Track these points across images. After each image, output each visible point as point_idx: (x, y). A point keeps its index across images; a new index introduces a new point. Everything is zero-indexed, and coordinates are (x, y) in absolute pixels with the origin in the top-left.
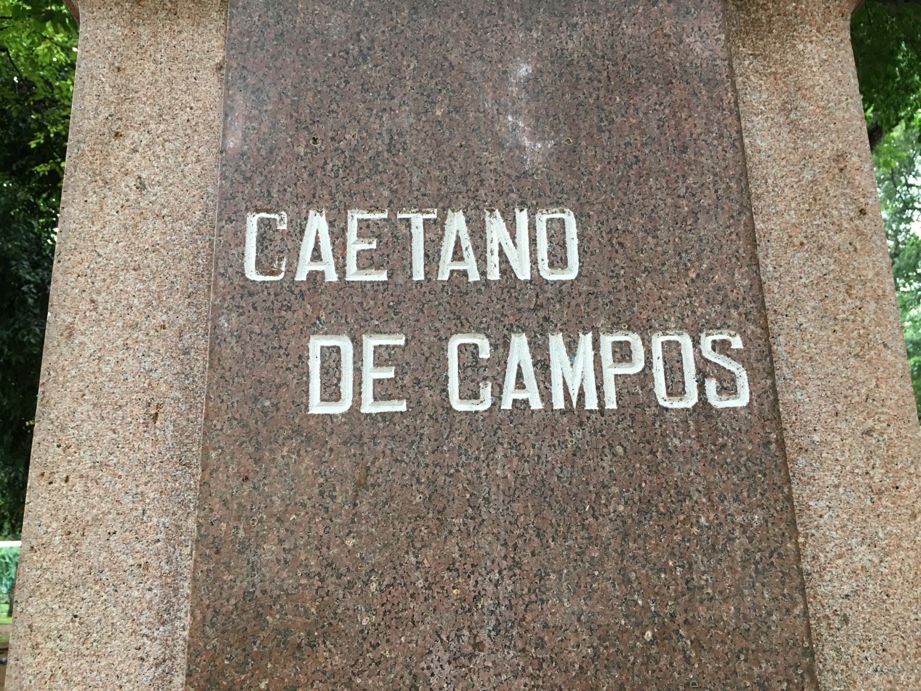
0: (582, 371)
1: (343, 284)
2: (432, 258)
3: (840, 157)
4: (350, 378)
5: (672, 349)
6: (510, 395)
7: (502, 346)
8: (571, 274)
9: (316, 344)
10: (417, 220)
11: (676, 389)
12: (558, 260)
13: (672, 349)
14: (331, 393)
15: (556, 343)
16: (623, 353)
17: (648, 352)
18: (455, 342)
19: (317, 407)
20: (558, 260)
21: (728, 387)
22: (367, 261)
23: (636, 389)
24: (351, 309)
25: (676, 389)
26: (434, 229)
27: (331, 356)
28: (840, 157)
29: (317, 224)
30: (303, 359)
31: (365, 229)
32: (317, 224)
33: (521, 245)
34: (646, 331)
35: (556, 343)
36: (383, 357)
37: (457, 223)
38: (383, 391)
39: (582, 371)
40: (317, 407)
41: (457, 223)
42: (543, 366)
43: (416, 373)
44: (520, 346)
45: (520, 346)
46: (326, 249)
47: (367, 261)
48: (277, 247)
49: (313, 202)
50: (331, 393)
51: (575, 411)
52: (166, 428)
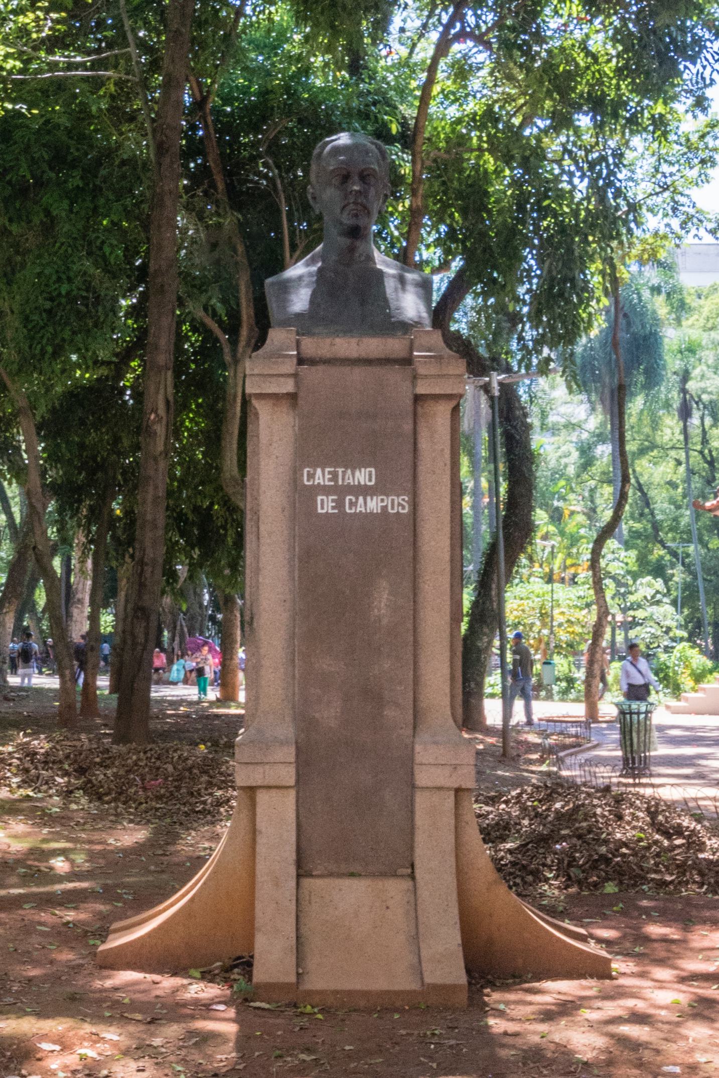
0: (374, 504)
1: (325, 486)
2: (343, 479)
3: (443, 450)
4: (326, 505)
5: (393, 500)
6: (358, 510)
7: (357, 499)
8: (373, 483)
9: (319, 498)
10: (340, 470)
11: (393, 508)
12: (370, 480)
13: (393, 500)
14: (322, 508)
15: (369, 498)
16: (382, 501)
17: (388, 501)
18: (348, 498)
19: (320, 511)
20: (370, 480)
21: (403, 508)
22: (330, 480)
23: (384, 508)
24: (326, 490)
25: (393, 508)
26: (344, 473)
27: (322, 500)
28: (443, 450)
29: (319, 471)
30: (316, 501)
31: (329, 473)
32: (319, 471)
33: (363, 476)
34: (387, 496)
35: (369, 498)
36: (333, 501)
37: (349, 471)
38: (333, 508)
39: (374, 504)
40: (320, 511)
41: (349, 471)
42: (365, 503)
43: (340, 504)
44: (361, 499)
45: (361, 499)
46: (321, 477)
47: (330, 480)
48: (311, 476)
49: (318, 466)
50: (322, 508)
51: (371, 513)
52: (286, 513)
